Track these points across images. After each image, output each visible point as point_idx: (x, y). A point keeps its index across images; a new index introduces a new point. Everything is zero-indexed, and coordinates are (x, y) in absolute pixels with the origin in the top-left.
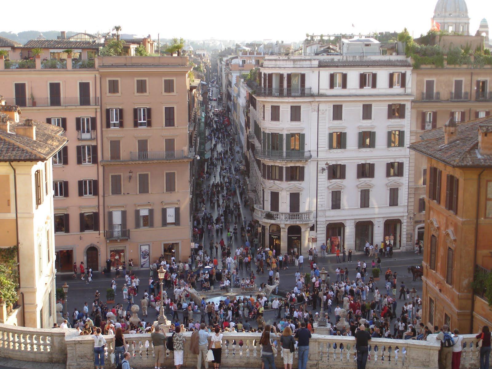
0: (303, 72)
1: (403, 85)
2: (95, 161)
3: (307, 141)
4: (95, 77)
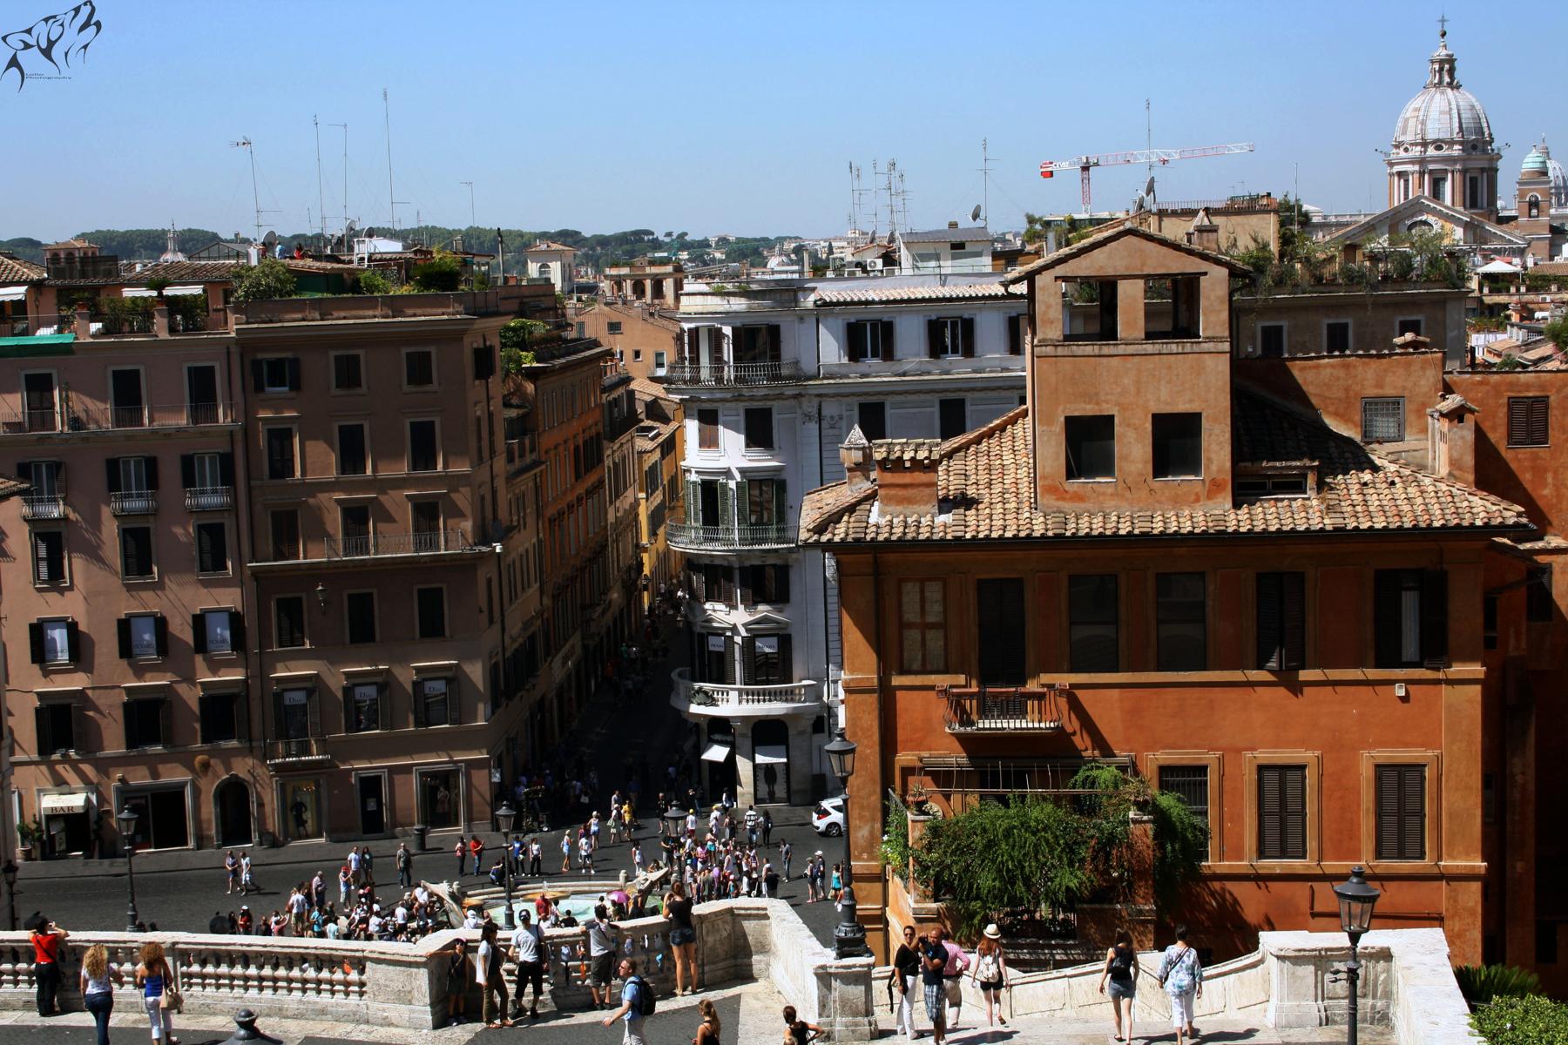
0: (773, 321)
4: (228, 353)
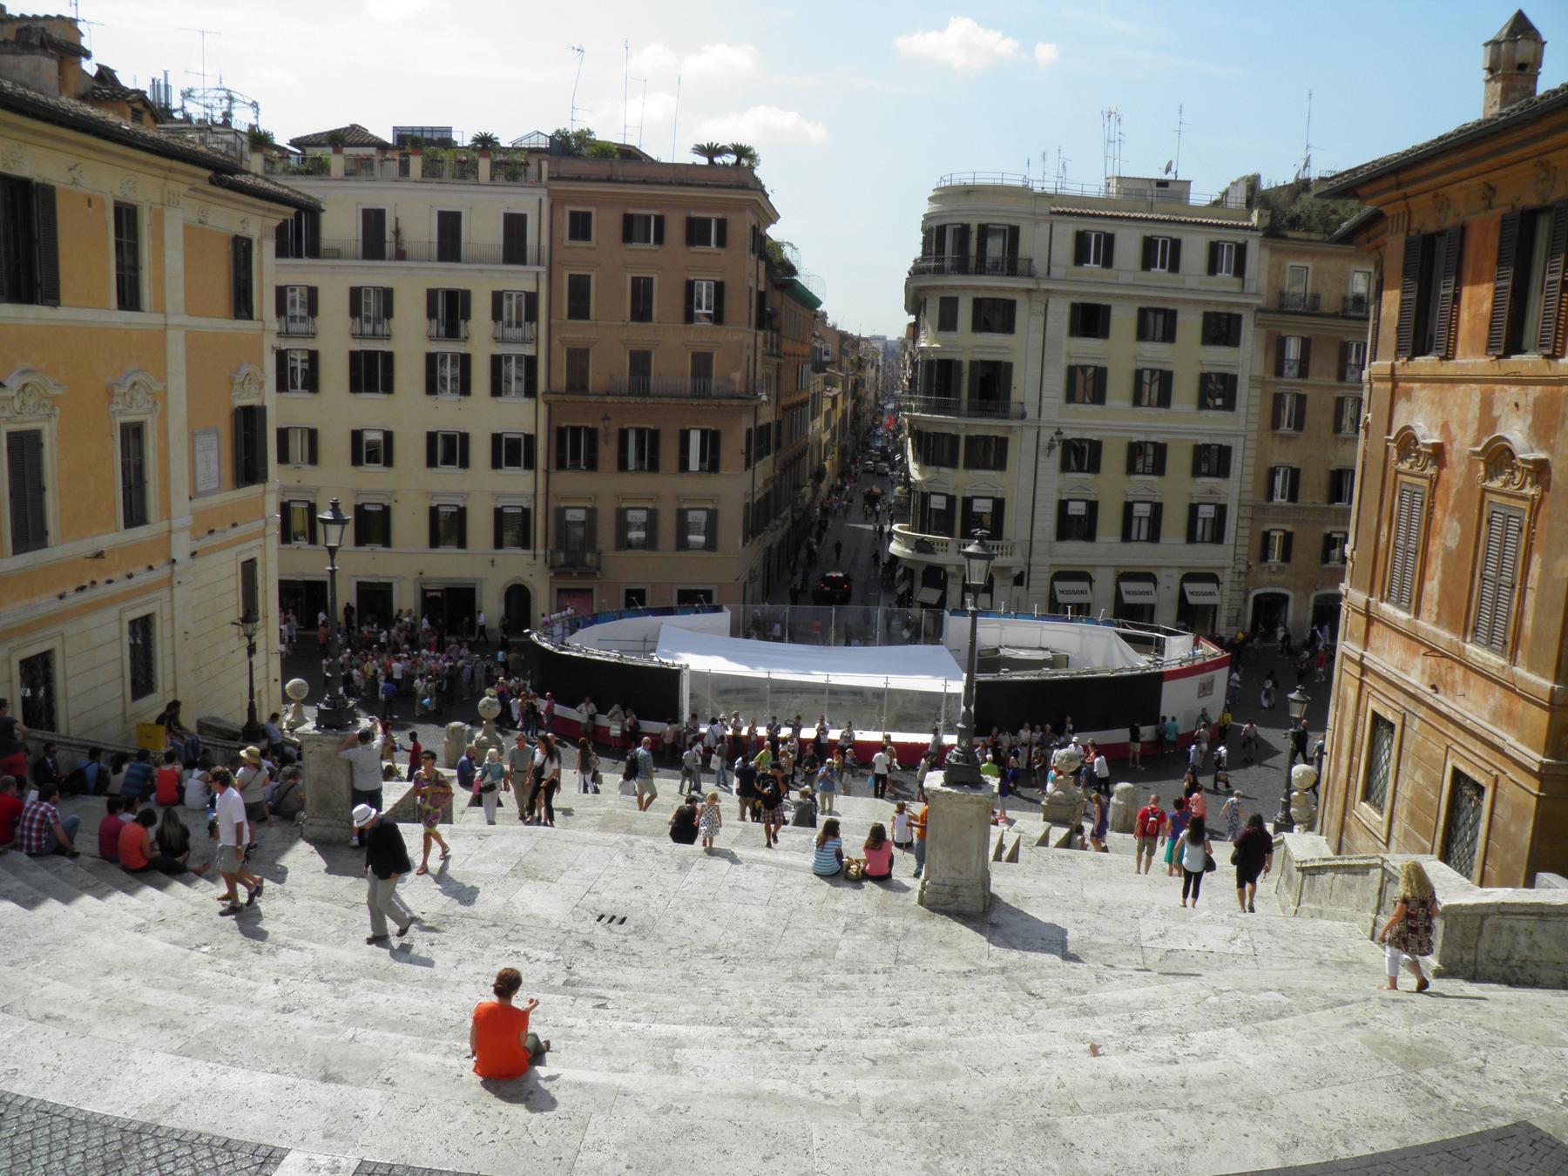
1: (1240, 270)
2: (530, 391)
3: (1017, 380)
